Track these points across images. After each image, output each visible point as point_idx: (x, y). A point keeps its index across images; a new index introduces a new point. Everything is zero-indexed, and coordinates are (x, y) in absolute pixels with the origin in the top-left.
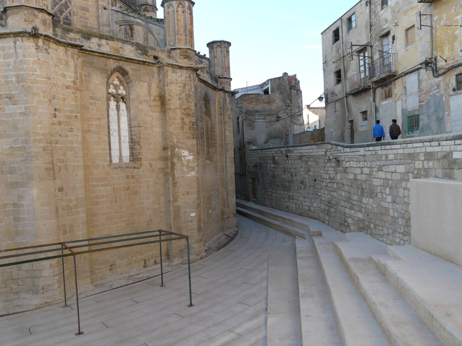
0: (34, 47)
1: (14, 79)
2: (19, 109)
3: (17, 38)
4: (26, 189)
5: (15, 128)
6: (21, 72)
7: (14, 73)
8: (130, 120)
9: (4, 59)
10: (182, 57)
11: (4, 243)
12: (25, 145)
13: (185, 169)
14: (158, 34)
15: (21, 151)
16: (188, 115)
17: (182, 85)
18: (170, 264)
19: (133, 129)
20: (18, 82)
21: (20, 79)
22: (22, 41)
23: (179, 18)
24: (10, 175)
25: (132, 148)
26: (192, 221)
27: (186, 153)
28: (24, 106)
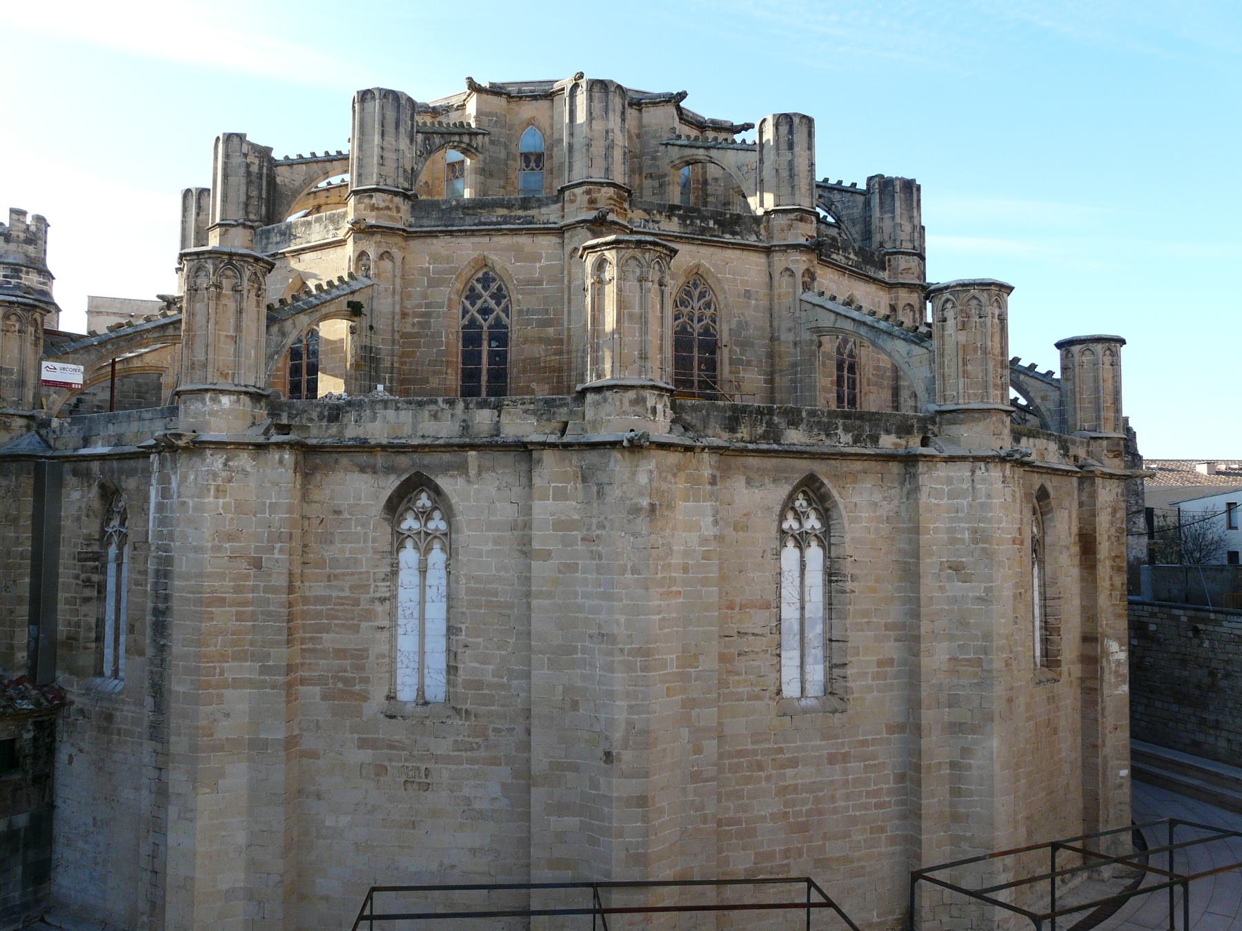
0: (1001, 479)
1: (967, 535)
3: (978, 464)
4: (979, 736)
5: (963, 623)
6: (982, 525)
7: (967, 525)
8: (1043, 585)
10: (1111, 455)
11: (935, 836)
12: (982, 657)
13: (1113, 680)
14: (1044, 398)
15: (973, 667)
16: (1119, 569)
17: (1109, 510)
18: (1095, 876)
19: (1049, 603)
20: (975, 541)
21: (979, 537)
22: (987, 470)
23: (1106, 376)
24: (947, 710)
25: (1045, 641)
26: (1121, 786)
27: (1114, 646)
28: (983, 585)
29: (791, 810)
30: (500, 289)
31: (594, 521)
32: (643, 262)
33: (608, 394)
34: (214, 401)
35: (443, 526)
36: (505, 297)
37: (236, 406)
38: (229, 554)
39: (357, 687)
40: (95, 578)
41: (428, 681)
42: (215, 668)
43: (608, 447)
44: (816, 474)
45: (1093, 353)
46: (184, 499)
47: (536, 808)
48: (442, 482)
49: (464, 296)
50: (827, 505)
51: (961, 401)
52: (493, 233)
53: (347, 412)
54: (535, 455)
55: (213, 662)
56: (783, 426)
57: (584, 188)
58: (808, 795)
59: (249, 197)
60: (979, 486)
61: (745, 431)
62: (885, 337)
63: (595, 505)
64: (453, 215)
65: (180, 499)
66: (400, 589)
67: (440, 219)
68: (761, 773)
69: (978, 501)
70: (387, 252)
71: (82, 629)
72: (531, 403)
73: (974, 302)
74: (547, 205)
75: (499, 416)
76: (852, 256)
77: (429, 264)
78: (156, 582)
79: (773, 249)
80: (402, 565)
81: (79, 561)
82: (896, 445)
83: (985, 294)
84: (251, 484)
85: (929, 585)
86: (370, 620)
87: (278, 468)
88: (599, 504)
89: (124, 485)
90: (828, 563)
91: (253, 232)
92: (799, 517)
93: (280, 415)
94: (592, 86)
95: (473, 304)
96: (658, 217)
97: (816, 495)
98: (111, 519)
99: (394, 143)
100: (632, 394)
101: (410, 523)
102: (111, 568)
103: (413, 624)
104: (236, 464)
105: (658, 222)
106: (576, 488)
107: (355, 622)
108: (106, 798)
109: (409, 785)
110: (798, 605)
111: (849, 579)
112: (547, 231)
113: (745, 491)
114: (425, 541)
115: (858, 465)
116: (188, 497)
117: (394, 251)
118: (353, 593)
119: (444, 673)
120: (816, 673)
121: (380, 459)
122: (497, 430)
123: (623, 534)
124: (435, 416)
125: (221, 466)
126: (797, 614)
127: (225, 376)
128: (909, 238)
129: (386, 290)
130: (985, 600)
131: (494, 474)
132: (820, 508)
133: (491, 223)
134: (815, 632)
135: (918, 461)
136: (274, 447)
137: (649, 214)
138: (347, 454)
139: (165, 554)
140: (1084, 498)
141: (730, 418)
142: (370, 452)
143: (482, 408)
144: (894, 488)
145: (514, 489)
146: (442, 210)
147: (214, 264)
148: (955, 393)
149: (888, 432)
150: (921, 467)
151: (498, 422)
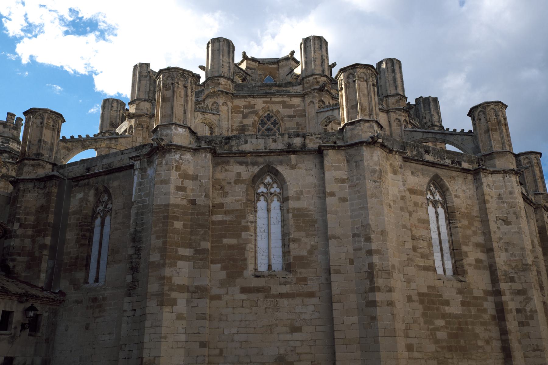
2: (513, 228)
3: (505, 174)
6: (511, 200)
9: (495, 190)
22: (510, 177)
29: (449, 326)
31: (355, 177)
33: (357, 124)
34: (176, 129)
35: (278, 190)
37: (185, 133)
38: (181, 197)
39: (240, 263)
40: (88, 234)
41: (273, 261)
42: (173, 249)
43: (360, 145)
44: (439, 174)
45: (529, 159)
47: (335, 313)
48: (279, 168)
49: (258, 123)
50: (444, 189)
51: (494, 149)
52: (272, 96)
53: (233, 140)
54: (325, 152)
55: (172, 246)
56: (423, 152)
58: (455, 320)
59: (150, 90)
60: (507, 184)
61: (408, 152)
62: (449, 136)
63: (355, 171)
64: (254, 89)
65: (157, 173)
66: (258, 219)
68: (434, 306)
69: (508, 190)
70: (225, 102)
73: (492, 111)
74: (296, 85)
75: (305, 140)
76: (417, 123)
77: (243, 109)
78: (136, 218)
79: (390, 110)
81: (79, 226)
82: (468, 167)
83: (497, 107)
84: (191, 167)
85: (493, 226)
86: (247, 232)
87: (204, 160)
88: (356, 170)
89: (110, 185)
90: (447, 216)
91: (151, 104)
92: (432, 194)
94: (314, 38)
95: (263, 127)
97: (438, 185)
98: (98, 206)
99: (227, 59)
100: (367, 124)
102: (97, 230)
103: (265, 235)
106: (344, 165)
107: (239, 232)
108: (89, 344)
109: (267, 309)
110: (437, 232)
111: (458, 222)
112: (297, 95)
113: (412, 177)
114: (268, 197)
115: (455, 174)
116: (161, 171)
117: (229, 103)
118: (237, 219)
119: (281, 257)
120: (449, 265)
121: (249, 159)
122: (304, 145)
123: (370, 181)
124: (275, 141)
126: (437, 237)
127: (180, 121)
128: (437, 121)
129: (225, 118)
130: (519, 233)
131: (303, 164)
132: (441, 191)
133: (272, 93)
134: (446, 246)
135: (479, 172)
136: (203, 150)
138: (234, 157)
139: (142, 204)
140: (538, 217)
141: (402, 146)
143: (296, 137)
144: (470, 185)
145: (313, 170)
146: (249, 87)
147: (176, 74)
148: (490, 148)
149: (465, 162)
150: (482, 175)
151: (304, 142)
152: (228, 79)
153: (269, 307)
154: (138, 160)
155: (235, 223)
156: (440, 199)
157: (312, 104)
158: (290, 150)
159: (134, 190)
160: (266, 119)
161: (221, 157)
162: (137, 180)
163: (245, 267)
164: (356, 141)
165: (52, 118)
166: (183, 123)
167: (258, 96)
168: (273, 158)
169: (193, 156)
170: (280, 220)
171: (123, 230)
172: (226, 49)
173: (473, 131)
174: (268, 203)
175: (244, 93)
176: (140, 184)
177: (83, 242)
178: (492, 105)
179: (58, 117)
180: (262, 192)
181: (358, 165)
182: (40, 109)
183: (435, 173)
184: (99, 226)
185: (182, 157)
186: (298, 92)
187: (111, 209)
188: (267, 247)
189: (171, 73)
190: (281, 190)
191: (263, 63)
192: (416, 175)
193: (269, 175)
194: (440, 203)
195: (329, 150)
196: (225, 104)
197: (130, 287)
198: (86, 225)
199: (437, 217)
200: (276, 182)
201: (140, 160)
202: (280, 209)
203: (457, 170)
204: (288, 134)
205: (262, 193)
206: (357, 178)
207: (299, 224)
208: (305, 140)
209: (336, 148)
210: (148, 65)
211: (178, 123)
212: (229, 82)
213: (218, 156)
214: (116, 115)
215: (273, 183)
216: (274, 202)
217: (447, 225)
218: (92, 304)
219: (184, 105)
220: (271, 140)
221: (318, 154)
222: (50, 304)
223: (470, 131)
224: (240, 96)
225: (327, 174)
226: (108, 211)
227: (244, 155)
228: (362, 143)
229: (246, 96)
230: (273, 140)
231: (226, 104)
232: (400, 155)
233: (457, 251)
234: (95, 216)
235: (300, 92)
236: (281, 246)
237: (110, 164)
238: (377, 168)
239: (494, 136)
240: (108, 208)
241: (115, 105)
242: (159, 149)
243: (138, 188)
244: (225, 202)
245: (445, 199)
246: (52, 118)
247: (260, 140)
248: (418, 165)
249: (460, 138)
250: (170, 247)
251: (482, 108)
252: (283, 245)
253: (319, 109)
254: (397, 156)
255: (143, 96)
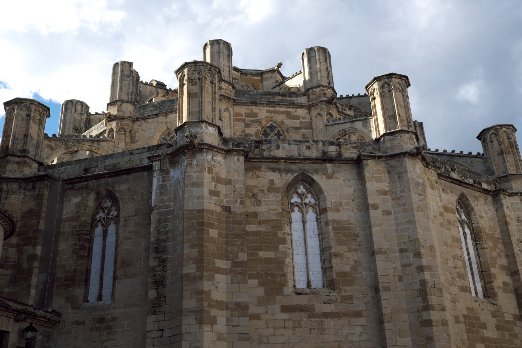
30: (279, 131)
31: (398, 190)
32: (402, 85)
33: (397, 135)
35: (313, 201)
36: (282, 135)
38: (215, 202)
40: (87, 245)
41: (312, 278)
42: (210, 260)
43: (402, 156)
46: (190, 174)
47: (388, 334)
48: (315, 177)
50: (469, 209)
51: (509, 172)
52: (276, 106)
53: (264, 144)
54: (365, 162)
55: (209, 257)
56: (450, 170)
57: (322, 88)
58: (493, 345)
59: (132, 91)
62: (457, 158)
63: (398, 183)
64: (256, 97)
65: (187, 174)
67: (250, 98)
71: (78, 274)
72: (354, 144)
73: (504, 134)
74: (300, 96)
75: (340, 149)
77: (245, 117)
78: (158, 226)
80: (293, 220)
81: (76, 235)
82: (487, 188)
88: (399, 182)
89: (117, 189)
90: (474, 236)
91: (134, 107)
93: (228, 144)
94: (319, 49)
96: (346, 109)
97: (463, 204)
98: (98, 213)
99: (227, 62)
100: (407, 135)
101: (295, 199)
103: (302, 249)
104: (217, 159)
105: (346, 110)
106: (385, 177)
107: (276, 245)
109: (312, 331)
114: (302, 207)
115: (477, 194)
116: (192, 172)
117: (231, 109)
119: (321, 273)
121: (282, 165)
122: (340, 154)
123: (415, 194)
124: (308, 148)
125: (210, 158)
127: (209, 119)
131: (341, 174)
133: (275, 102)
134: (475, 267)
135: (499, 193)
136: (235, 153)
137: (342, 106)
138: (265, 163)
139: (165, 210)
142: (277, 162)
143: (331, 145)
145: (351, 181)
146: (250, 95)
150: (502, 196)
151: (340, 151)
152: (230, 83)
153: (314, 327)
154: (158, 160)
155: (271, 235)
156: (466, 219)
157: (319, 117)
158: (325, 159)
159: (154, 193)
160: (269, 129)
161: (251, 161)
162: (157, 183)
163: (285, 284)
164: (397, 151)
165: (39, 111)
166: (212, 122)
167: (261, 104)
168: (307, 166)
169: (225, 158)
170: (317, 233)
171: (135, 240)
172: (226, 52)
173: (482, 152)
174: (303, 214)
175: (246, 100)
176: (161, 187)
177: (82, 253)
178: (504, 128)
179: (45, 111)
180: (296, 202)
181: (401, 177)
182: (26, 100)
183: (461, 192)
184: (101, 236)
185: (214, 158)
186: (303, 103)
187: (118, 216)
188: (305, 262)
189: (197, 67)
190: (317, 201)
191: (245, 74)
192: (446, 192)
193: (302, 184)
194: (466, 223)
195: (369, 159)
196: (226, 110)
197: (155, 304)
198: (85, 234)
199: (465, 237)
200: (310, 192)
201: (160, 160)
202: (317, 221)
203: (480, 190)
204: (322, 141)
205: (297, 204)
206: (401, 190)
207: (340, 238)
208: (340, 149)
209: (376, 158)
210: (130, 64)
211: (207, 120)
212: (230, 87)
213: (249, 161)
214: (79, 119)
215: (308, 193)
216: (309, 213)
217: (474, 246)
218: (98, 325)
219: (212, 103)
220: (304, 147)
221: (355, 164)
222: (45, 325)
223: (479, 154)
224: (241, 103)
225: (369, 185)
226: (112, 219)
227: (276, 161)
228: (404, 154)
229: (248, 103)
230: (307, 147)
231: (227, 110)
232: (435, 170)
233: (486, 272)
234: (96, 224)
235: (305, 103)
236: (320, 261)
237: (116, 164)
238: (421, 181)
239: (508, 159)
240: (112, 215)
241: (79, 107)
242: (189, 148)
243: (158, 192)
244: (258, 211)
245: (471, 219)
246: (39, 111)
247: (293, 146)
248: (447, 182)
249: (469, 160)
250: (207, 258)
251: (494, 130)
252: (323, 261)
253: (327, 122)
254: (432, 171)
255: (125, 98)
